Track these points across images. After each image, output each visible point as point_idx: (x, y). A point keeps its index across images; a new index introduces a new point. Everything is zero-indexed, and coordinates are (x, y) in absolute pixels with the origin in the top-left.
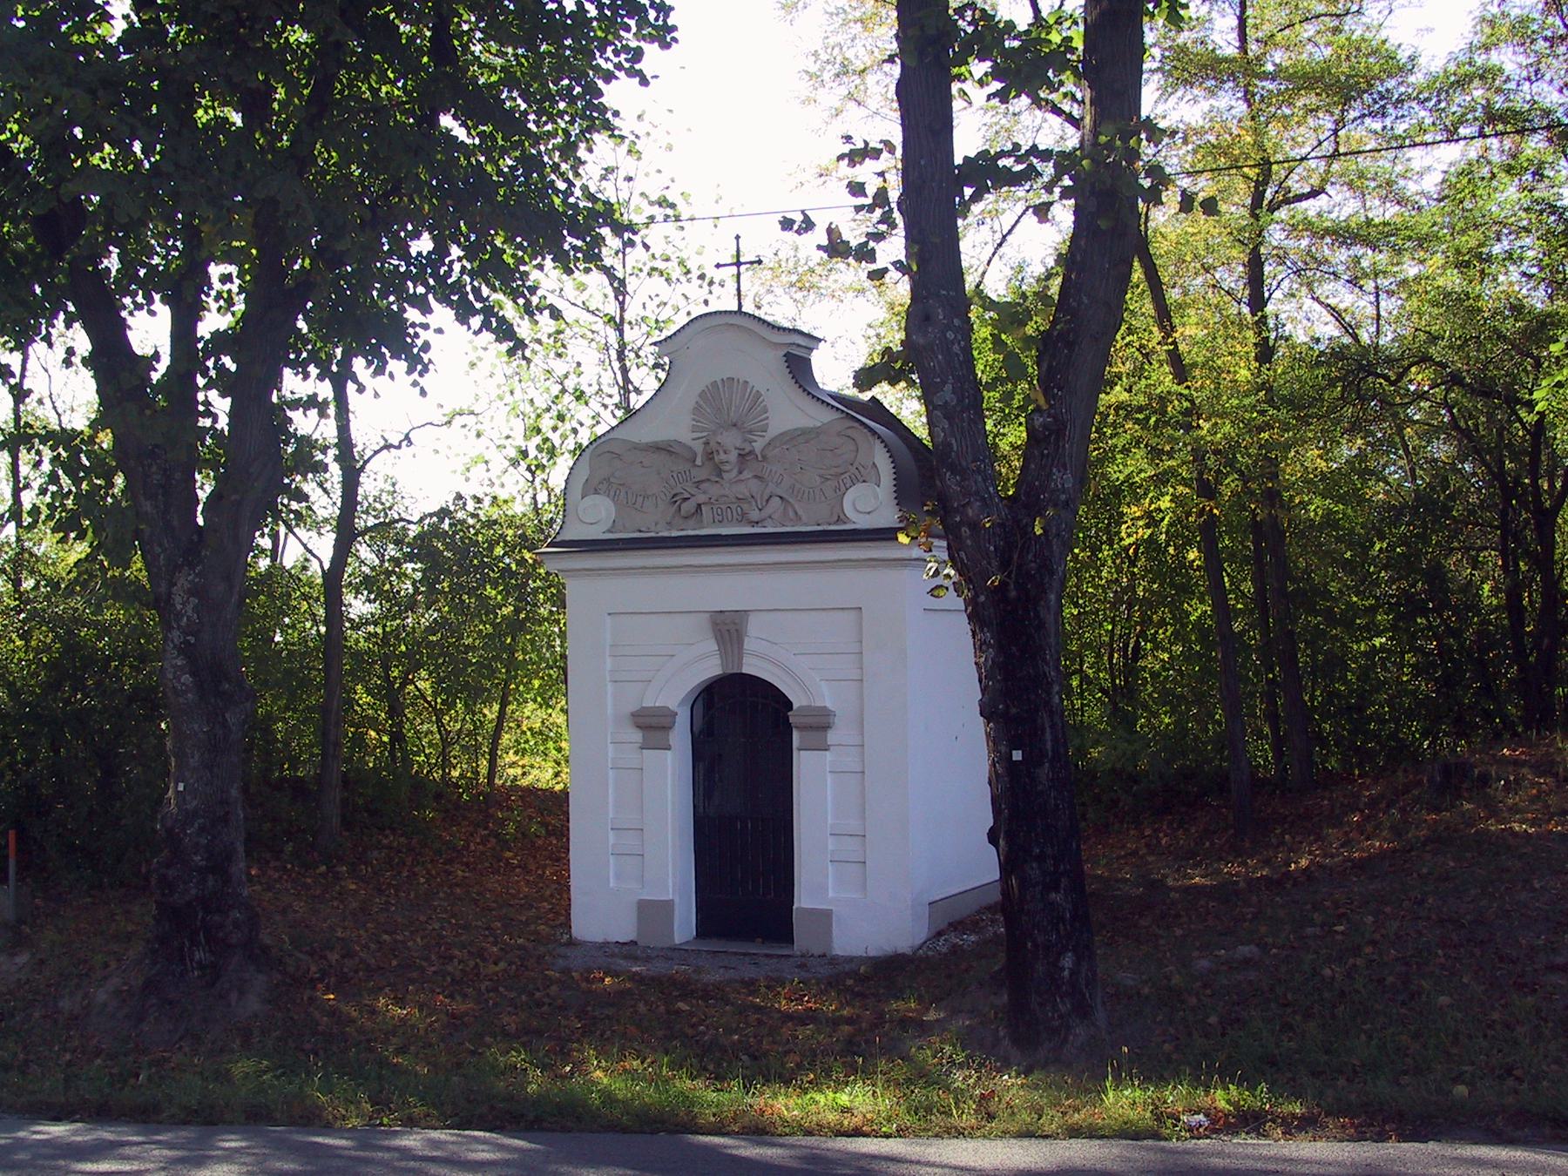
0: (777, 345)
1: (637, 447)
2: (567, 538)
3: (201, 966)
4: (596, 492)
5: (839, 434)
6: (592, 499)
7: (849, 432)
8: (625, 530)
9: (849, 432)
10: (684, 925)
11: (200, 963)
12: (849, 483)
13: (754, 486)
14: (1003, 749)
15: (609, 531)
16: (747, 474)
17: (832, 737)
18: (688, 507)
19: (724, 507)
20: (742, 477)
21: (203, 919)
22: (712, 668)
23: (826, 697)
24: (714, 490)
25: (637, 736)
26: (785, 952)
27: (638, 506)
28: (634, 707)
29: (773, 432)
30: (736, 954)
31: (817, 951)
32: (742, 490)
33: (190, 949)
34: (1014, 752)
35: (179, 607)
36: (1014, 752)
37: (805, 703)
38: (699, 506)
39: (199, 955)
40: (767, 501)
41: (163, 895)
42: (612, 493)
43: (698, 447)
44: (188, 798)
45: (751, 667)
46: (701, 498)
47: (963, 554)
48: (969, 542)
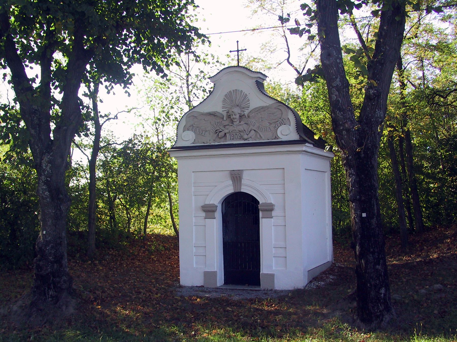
0: (252, 78)
1: (203, 114)
2: (178, 146)
3: (52, 297)
4: (188, 130)
5: (275, 108)
6: (187, 132)
7: (279, 107)
8: (198, 143)
9: (279, 107)
10: (220, 280)
11: (51, 295)
12: (279, 125)
13: (245, 127)
14: (358, 213)
15: (193, 143)
16: (242, 123)
17: (274, 213)
18: (221, 134)
19: (234, 134)
20: (240, 124)
21: (53, 280)
22: (230, 190)
23: (271, 200)
24: (231, 128)
25: (204, 214)
26: (258, 289)
27: (203, 134)
28: (202, 204)
29: (250, 109)
30: (240, 290)
31: (269, 289)
32: (241, 128)
33: (48, 290)
35: (44, 168)
37: (264, 202)
38: (225, 134)
39: (51, 293)
40: (250, 132)
41: (38, 271)
42: (194, 130)
43: (225, 114)
44: (47, 236)
45: (244, 189)
46: (226, 131)
47: (343, 141)
48: (346, 137)
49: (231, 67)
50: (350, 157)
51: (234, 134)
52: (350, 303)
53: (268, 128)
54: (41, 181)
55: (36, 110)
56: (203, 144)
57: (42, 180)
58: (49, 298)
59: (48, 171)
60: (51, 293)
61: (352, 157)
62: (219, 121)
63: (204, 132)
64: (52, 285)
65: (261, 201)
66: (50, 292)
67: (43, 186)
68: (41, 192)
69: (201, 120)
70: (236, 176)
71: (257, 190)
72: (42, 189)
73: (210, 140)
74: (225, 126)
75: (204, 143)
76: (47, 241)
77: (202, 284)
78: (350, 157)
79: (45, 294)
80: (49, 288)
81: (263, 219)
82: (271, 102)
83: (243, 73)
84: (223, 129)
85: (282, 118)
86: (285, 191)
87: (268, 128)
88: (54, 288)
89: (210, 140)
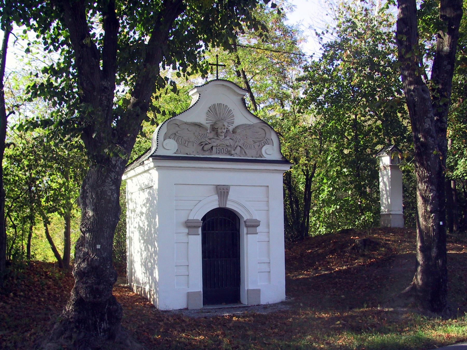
0: (239, 94)
1: (186, 123)
2: (158, 154)
3: (104, 331)
4: (170, 138)
5: (259, 128)
6: (168, 141)
7: (264, 128)
8: (181, 153)
9: (264, 128)
11: (104, 329)
12: (263, 144)
13: (232, 142)
14: (437, 221)
15: (175, 153)
16: (228, 138)
17: (259, 229)
18: (206, 147)
19: (221, 148)
20: (226, 138)
21: (108, 308)
22: (215, 205)
23: (257, 216)
24: (218, 142)
25: (186, 230)
26: (238, 306)
27: (186, 145)
28: (185, 219)
29: (235, 125)
30: (227, 308)
31: (256, 304)
32: (227, 143)
33: (99, 323)
34: (99, 248)
35: (114, 162)
36: (99, 248)
37: (249, 217)
38: (212, 147)
39: (104, 325)
40: (236, 148)
41: (95, 297)
42: (176, 139)
43: (208, 126)
44: (102, 251)
45: (230, 205)
46: (215, 144)
47: (429, 163)
48: (433, 159)
49: (226, 80)
50: (433, 176)
51: (221, 148)
52: (406, 299)
53: (252, 146)
54: (110, 180)
55: (106, 88)
56: (186, 155)
57: (111, 178)
58: (101, 332)
59: (119, 167)
60: (104, 325)
61: (435, 176)
62: (203, 132)
63: (187, 142)
64: (106, 315)
65: (245, 216)
66: (103, 325)
67: (111, 186)
68: (110, 194)
69: (184, 129)
70: (224, 191)
71: (243, 207)
72: (111, 189)
73: (193, 152)
74: (210, 139)
75: (187, 154)
76: (103, 258)
77: (185, 306)
78: (433, 176)
79: (96, 328)
80: (102, 320)
81: (248, 235)
82: (255, 121)
83: (229, 88)
84: (210, 142)
85: (266, 138)
86: (269, 208)
87: (252, 146)
88: (108, 319)
89: (193, 152)
